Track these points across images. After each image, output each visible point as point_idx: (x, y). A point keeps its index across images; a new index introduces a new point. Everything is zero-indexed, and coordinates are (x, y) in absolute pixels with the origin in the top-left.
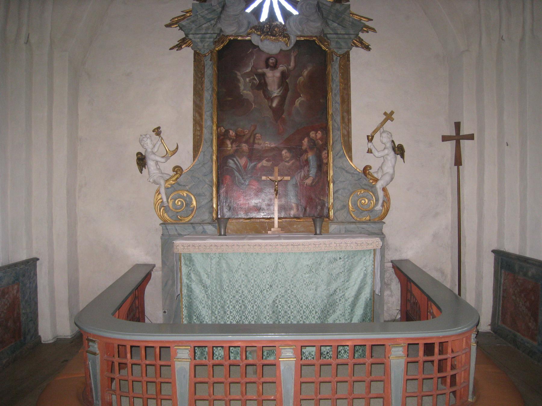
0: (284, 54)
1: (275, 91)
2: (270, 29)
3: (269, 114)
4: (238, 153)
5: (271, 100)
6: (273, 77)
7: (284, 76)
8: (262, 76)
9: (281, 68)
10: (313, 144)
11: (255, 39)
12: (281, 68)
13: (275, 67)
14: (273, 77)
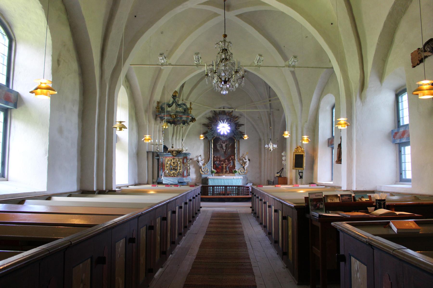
0: (226, 140)
1: (224, 148)
2: (224, 135)
3: (223, 153)
4: (217, 160)
5: (223, 150)
6: (224, 145)
7: (226, 145)
8: (222, 145)
9: (226, 143)
10: (232, 159)
11: (220, 138)
12: (226, 143)
13: (224, 143)
14: (224, 145)
